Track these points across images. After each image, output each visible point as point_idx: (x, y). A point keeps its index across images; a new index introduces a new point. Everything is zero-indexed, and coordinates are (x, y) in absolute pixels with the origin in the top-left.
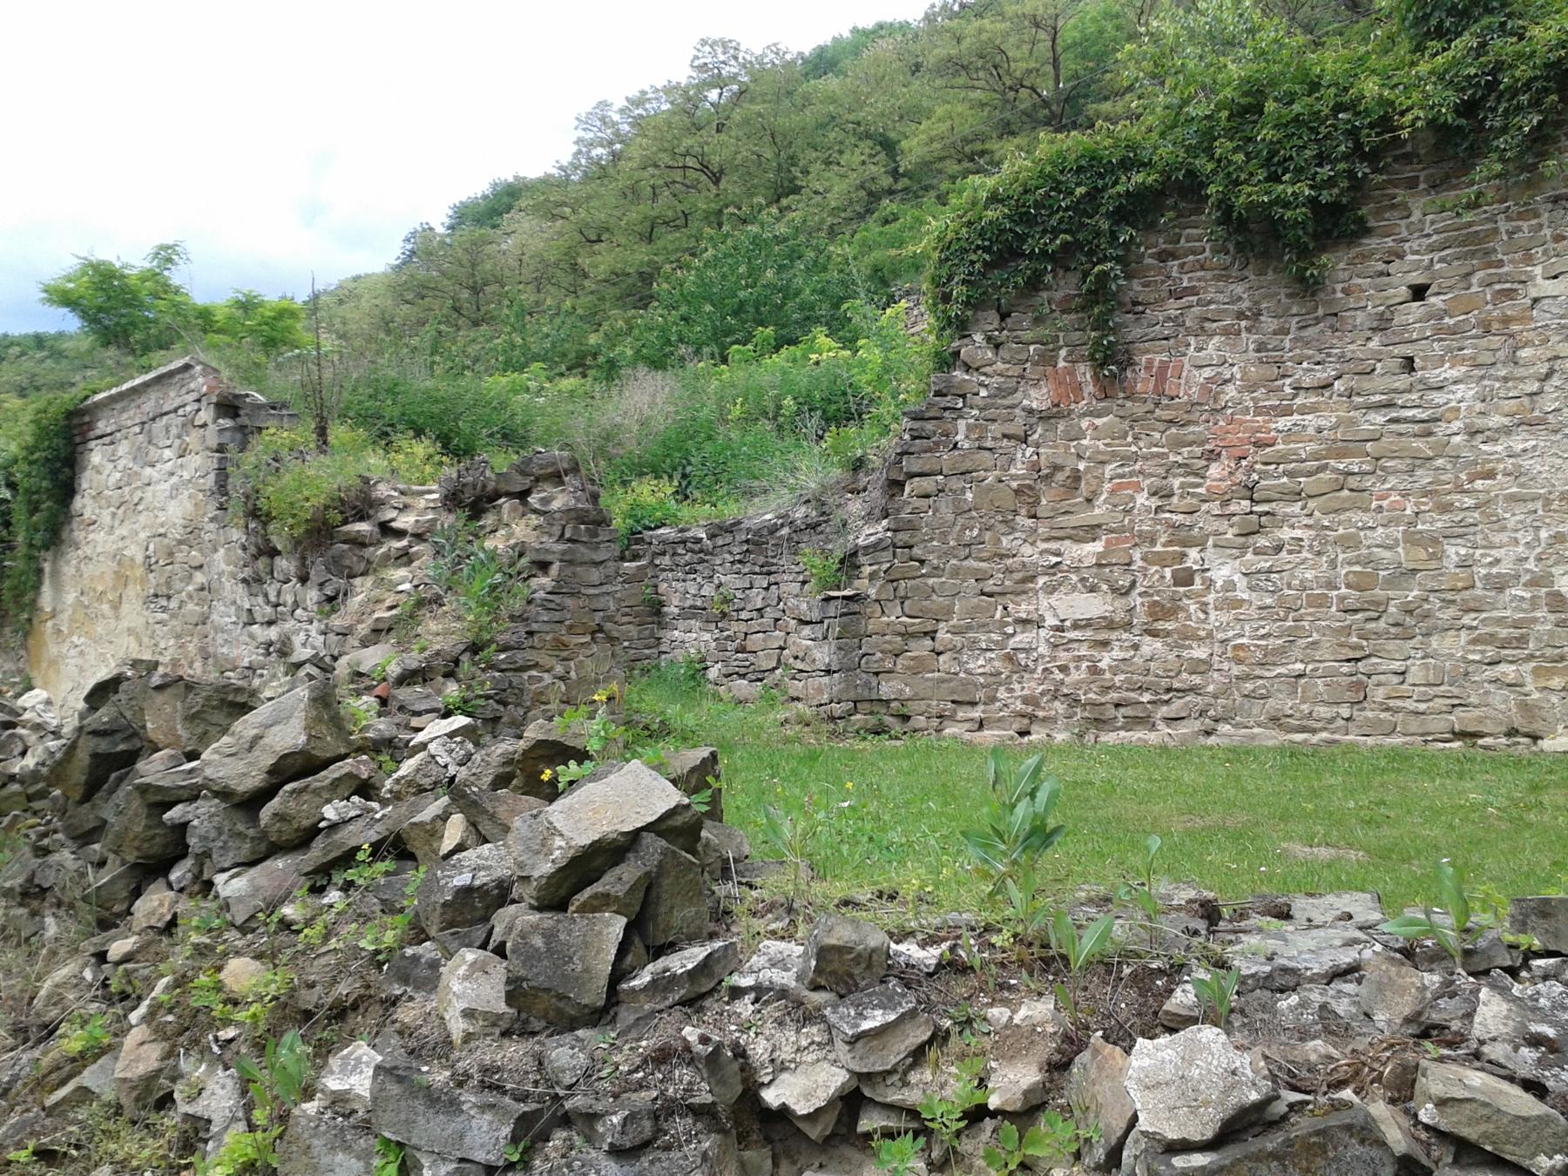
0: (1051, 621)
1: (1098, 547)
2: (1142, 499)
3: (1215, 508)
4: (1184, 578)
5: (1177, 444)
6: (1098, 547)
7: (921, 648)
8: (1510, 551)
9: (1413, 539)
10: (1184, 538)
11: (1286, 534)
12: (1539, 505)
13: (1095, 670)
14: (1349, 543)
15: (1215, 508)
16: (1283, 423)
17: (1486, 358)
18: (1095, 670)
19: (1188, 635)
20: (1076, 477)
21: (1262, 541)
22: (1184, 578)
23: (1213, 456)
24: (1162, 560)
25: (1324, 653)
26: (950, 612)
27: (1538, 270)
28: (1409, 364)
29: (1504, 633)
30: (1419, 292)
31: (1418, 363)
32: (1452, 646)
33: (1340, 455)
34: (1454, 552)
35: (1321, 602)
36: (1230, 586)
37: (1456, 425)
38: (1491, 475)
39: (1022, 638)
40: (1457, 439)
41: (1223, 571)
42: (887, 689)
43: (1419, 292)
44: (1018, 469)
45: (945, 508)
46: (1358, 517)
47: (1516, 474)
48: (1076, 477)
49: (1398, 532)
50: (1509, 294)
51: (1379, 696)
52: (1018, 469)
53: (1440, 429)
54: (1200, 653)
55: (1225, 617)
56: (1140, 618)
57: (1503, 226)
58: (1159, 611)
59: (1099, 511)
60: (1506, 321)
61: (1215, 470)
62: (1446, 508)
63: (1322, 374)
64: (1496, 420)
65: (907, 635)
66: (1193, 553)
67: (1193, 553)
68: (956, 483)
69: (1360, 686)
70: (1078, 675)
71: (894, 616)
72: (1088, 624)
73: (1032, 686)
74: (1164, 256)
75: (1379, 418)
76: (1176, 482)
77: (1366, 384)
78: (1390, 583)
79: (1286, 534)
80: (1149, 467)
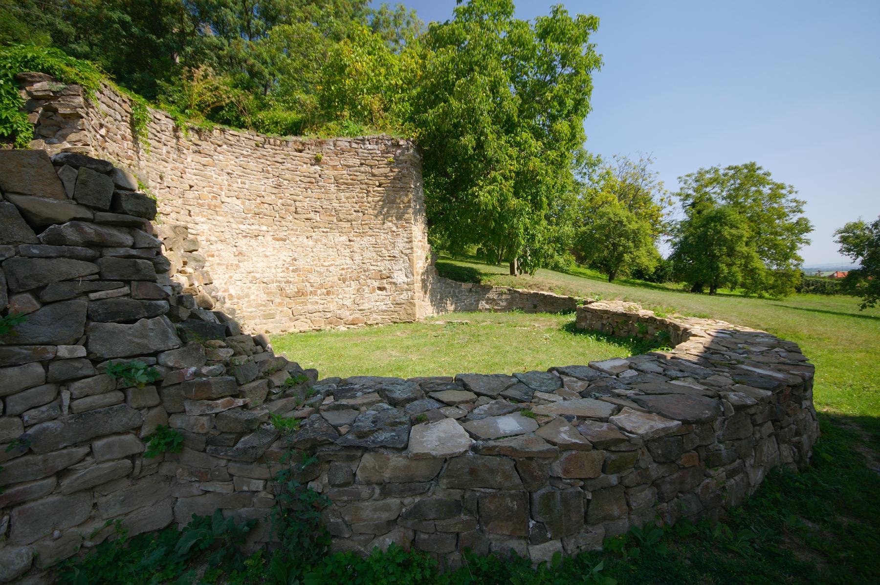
12: (224, 267)
17: (210, 217)
27: (223, 193)
31: (192, 213)
37: (204, 238)
38: (213, 256)
40: (203, 243)
50: (215, 198)
57: (214, 176)
60: (215, 206)
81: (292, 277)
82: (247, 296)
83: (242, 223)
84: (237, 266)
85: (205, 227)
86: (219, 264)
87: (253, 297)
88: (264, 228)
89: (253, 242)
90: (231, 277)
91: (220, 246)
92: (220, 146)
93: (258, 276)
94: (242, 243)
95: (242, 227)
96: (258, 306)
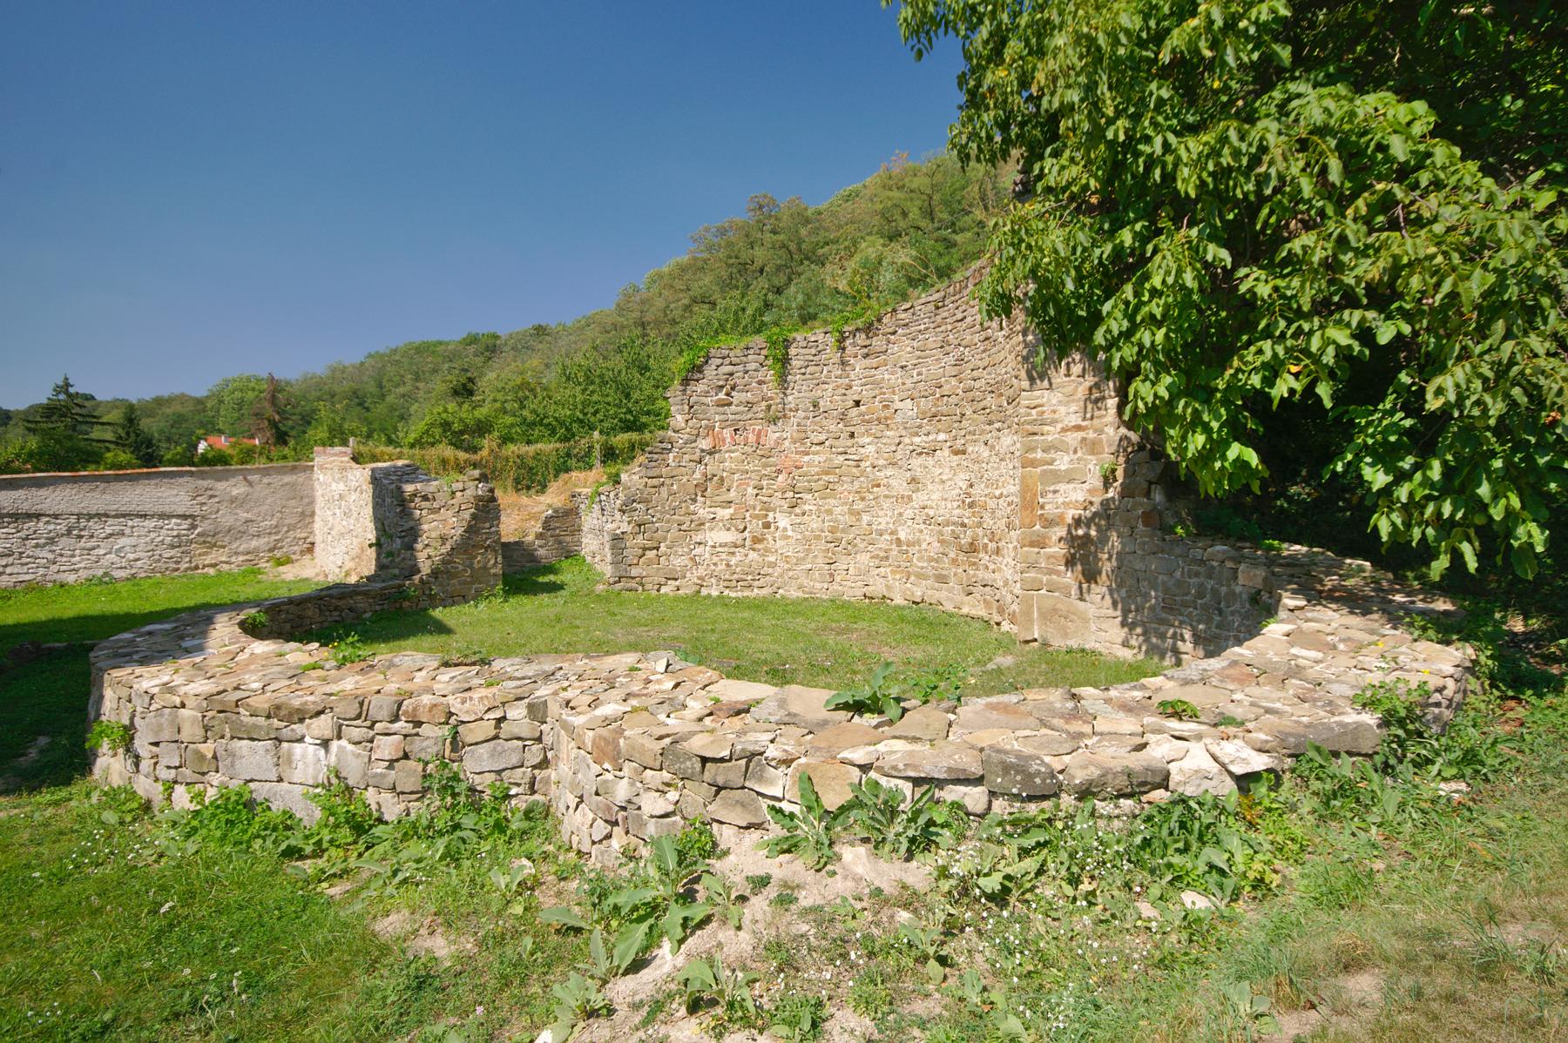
0: (711, 543)
1: (731, 511)
2: (750, 490)
3: (779, 494)
4: (767, 526)
5: (765, 466)
6: (731, 511)
7: (651, 554)
8: (884, 521)
9: (851, 512)
10: (767, 508)
11: (806, 507)
13: (728, 565)
14: (829, 512)
15: (779, 494)
16: (806, 458)
18: (728, 565)
19: (767, 550)
20: (722, 479)
21: (797, 510)
22: (767, 526)
23: (779, 472)
24: (757, 517)
25: (820, 560)
26: (665, 539)
28: (852, 435)
29: (882, 554)
30: (857, 403)
32: (864, 558)
33: (827, 473)
34: (865, 518)
35: (818, 538)
36: (785, 529)
38: (878, 486)
39: (698, 550)
41: (783, 521)
42: (634, 572)
43: (857, 403)
44: (697, 475)
45: (664, 491)
46: (832, 501)
47: (888, 486)
48: (722, 479)
49: (846, 508)
50: (887, 407)
51: (838, 579)
52: (697, 475)
53: (863, 464)
54: (772, 559)
55: (782, 543)
56: (748, 543)
58: (756, 540)
59: (732, 494)
61: (781, 478)
62: (863, 499)
63: (822, 437)
64: (881, 462)
65: (645, 549)
66: (771, 515)
67: (771, 515)
68: (668, 481)
69: (832, 575)
70: (722, 567)
71: (640, 540)
72: (726, 545)
73: (701, 571)
74: (760, 383)
75: (841, 458)
76: (764, 483)
77: (836, 443)
78: (843, 531)
79: (806, 507)
80: (753, 476)
81: (967, 516)
82: (919, 542)
83: (917, 434)
84: (910, 498)
85: (871, 449)
86: (886, 496)
87: (924, 546)
88: (942, 436)
89: (931, 461)
90: (900, 514)
91: (889, 472)
92: (894, 333)
93: (931, 513)
94: (916, 462)
95: (917, 440)
96: (931, 560)
